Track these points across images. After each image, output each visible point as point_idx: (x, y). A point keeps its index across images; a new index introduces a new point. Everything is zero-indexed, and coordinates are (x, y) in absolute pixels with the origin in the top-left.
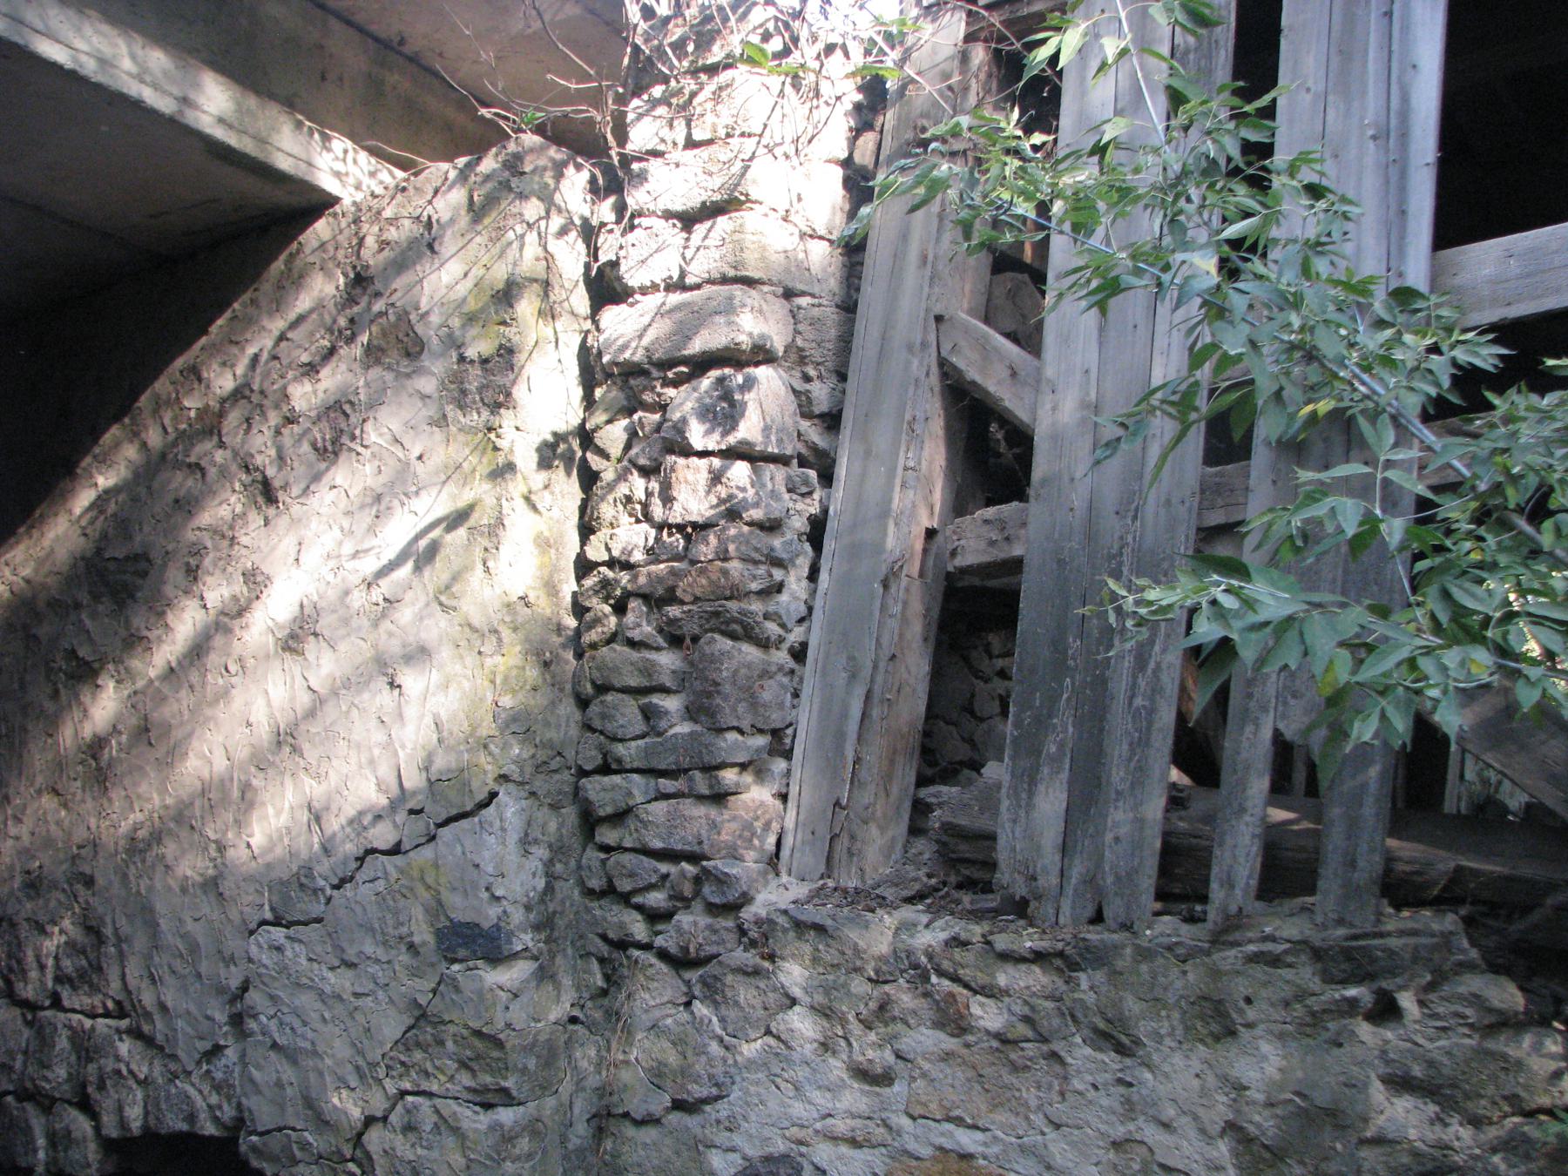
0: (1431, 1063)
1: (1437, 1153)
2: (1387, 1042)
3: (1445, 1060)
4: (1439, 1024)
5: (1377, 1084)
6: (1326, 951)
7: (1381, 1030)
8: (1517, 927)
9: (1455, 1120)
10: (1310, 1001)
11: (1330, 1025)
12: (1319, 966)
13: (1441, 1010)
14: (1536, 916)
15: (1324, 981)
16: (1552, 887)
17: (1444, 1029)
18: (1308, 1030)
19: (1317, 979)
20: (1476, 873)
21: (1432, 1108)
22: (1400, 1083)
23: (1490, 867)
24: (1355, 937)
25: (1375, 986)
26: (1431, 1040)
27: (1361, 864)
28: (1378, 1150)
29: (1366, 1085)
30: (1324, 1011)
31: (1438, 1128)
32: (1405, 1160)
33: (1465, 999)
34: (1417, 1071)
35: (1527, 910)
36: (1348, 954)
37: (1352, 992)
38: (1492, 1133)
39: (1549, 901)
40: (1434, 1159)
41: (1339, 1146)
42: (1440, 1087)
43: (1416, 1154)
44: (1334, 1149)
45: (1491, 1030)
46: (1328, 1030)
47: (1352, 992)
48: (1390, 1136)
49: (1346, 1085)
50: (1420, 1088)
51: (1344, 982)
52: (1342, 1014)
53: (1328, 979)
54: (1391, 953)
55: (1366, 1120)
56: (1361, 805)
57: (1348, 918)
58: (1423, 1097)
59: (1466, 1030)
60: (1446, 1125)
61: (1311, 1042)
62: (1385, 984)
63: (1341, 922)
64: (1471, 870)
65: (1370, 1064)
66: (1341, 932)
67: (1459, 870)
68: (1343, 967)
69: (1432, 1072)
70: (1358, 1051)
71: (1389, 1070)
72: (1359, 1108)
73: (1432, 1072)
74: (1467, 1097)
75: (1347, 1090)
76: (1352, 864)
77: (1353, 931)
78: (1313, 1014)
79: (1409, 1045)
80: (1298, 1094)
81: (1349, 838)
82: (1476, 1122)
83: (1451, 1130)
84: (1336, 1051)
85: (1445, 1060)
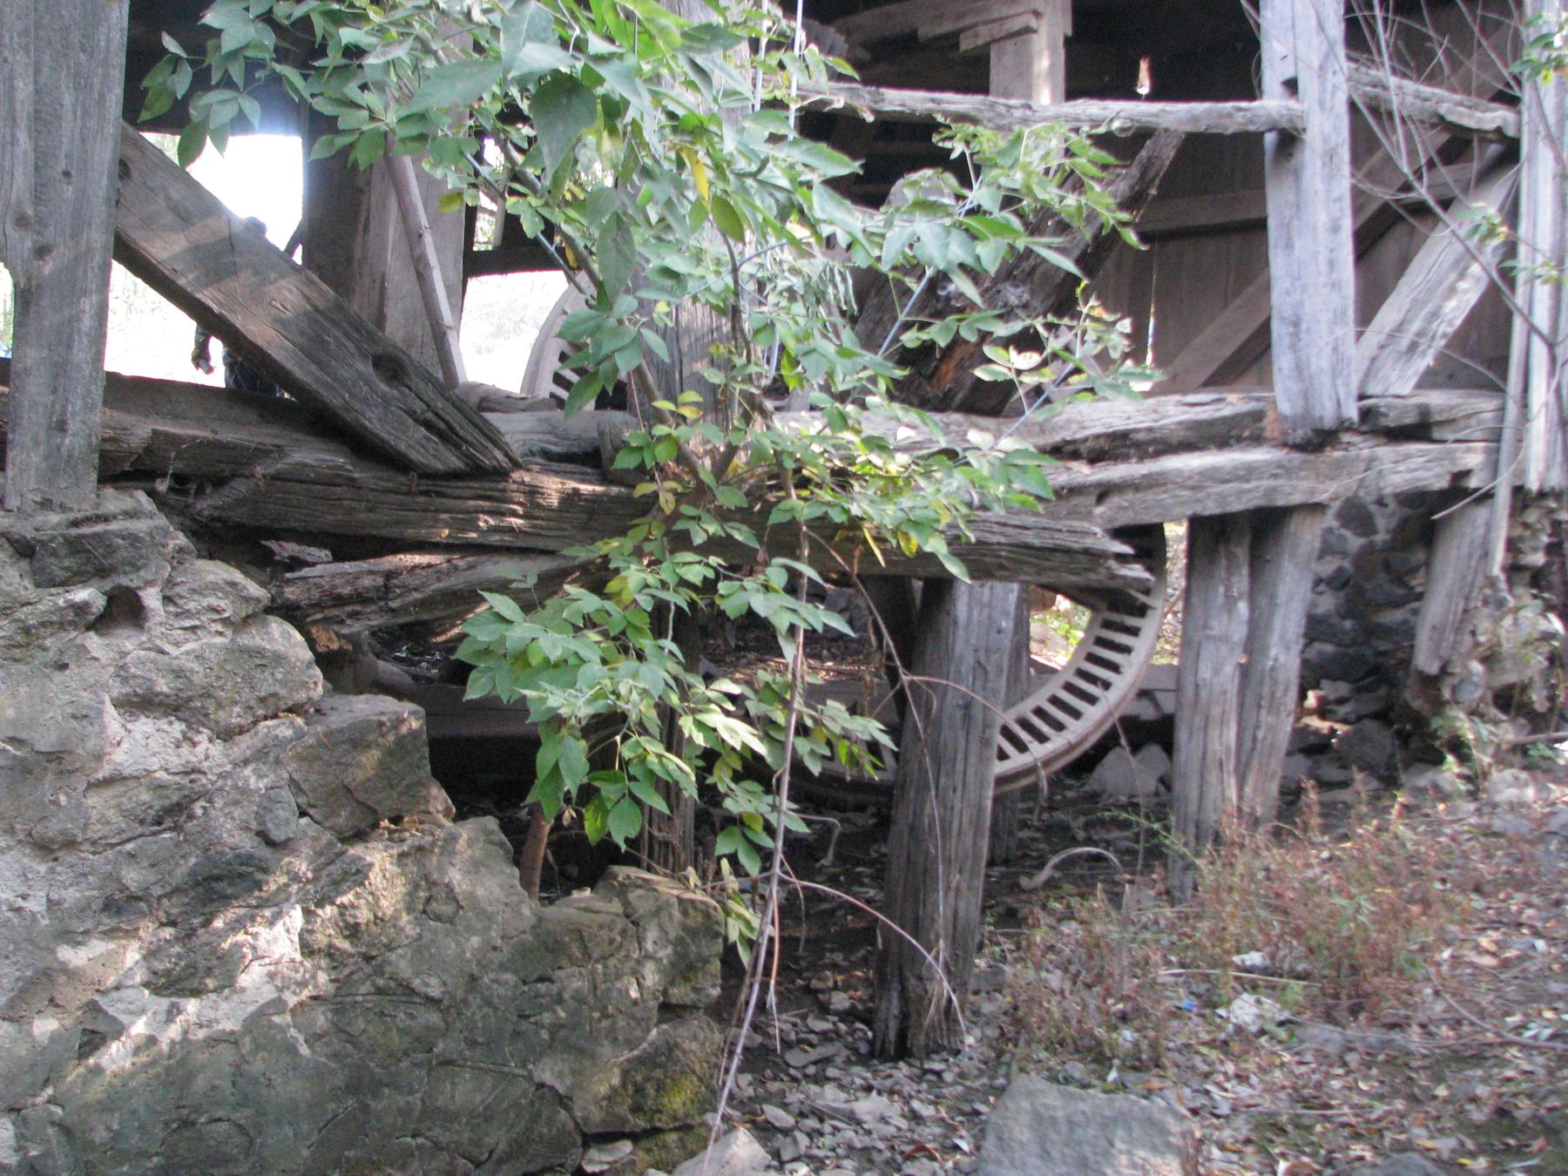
0: (179, 673)
1: (185, 781)
2: (124, 654)
3: (195, 666)
4: (188, 623)
5: (110, 710)
6: (43, 543)
7: (113, 641)
8: (207, 505)
9: (203, 737)
10: (21, 614)
11: (48, 643)
12: (24, 564)
13: (192, 606)
14: (240, 487)
15: (38, 585)
16: (262, 453)
17: (193, 629)
18: (18, 653)
19: (27, 583)
20: (174, 440)
21: (178, 728)
22: (140, 703)
23: (191, 432)
24: (75, 524)
25: (108, 584)
26: (177, 644)
27: (73, 426)
28: (108, 793)
29: (100, 713)
30: (43, 624)
31: (185, 749)
32: (145, 797)
33: (222, 590)
34: (163, 686)
35: (219, 482)
36: (75, 546)
37: (81, 595)
38: (245, 744)
39: (259, 470)
40: (180, 788)
41: (63, 799)
42: (190, 699)
43: (160, 787)
44: (56, 803)
45: (242, 624)
46: (45, 649)
47: (81, 595)
48: (126, 772)
49: (74, 717)
50: (161, 704)
51: (65, 583)
52: (62, 626)
53: (45, 581)
54: (133, 539)
55: (99, 757)
56: (69, 347)
57: (57, 499)
58: (167, 715)
59: (219, 627)
60: (195, 744)
61: (23, 668)
62: (125, 581)
63: (46, 504)
64: (166, 434)
65: (106, 687)
66: (54, 518)
67: (155, 432)
68: (66, 563)
69: (179, 684)
70: (89, 673)
71: (128, 690)
72: (91, 744)
73: (179, 684)
74: (220, 706)
75: (74, 723)
76: (61, 427)
77: (72, 516)
78: (27, 631)
79: (152, 654)
80: (13, 740)
81: (55, 391)
82: (227, 735)
83: (201, 749)
84: (58, 677)
85: (195, 666)
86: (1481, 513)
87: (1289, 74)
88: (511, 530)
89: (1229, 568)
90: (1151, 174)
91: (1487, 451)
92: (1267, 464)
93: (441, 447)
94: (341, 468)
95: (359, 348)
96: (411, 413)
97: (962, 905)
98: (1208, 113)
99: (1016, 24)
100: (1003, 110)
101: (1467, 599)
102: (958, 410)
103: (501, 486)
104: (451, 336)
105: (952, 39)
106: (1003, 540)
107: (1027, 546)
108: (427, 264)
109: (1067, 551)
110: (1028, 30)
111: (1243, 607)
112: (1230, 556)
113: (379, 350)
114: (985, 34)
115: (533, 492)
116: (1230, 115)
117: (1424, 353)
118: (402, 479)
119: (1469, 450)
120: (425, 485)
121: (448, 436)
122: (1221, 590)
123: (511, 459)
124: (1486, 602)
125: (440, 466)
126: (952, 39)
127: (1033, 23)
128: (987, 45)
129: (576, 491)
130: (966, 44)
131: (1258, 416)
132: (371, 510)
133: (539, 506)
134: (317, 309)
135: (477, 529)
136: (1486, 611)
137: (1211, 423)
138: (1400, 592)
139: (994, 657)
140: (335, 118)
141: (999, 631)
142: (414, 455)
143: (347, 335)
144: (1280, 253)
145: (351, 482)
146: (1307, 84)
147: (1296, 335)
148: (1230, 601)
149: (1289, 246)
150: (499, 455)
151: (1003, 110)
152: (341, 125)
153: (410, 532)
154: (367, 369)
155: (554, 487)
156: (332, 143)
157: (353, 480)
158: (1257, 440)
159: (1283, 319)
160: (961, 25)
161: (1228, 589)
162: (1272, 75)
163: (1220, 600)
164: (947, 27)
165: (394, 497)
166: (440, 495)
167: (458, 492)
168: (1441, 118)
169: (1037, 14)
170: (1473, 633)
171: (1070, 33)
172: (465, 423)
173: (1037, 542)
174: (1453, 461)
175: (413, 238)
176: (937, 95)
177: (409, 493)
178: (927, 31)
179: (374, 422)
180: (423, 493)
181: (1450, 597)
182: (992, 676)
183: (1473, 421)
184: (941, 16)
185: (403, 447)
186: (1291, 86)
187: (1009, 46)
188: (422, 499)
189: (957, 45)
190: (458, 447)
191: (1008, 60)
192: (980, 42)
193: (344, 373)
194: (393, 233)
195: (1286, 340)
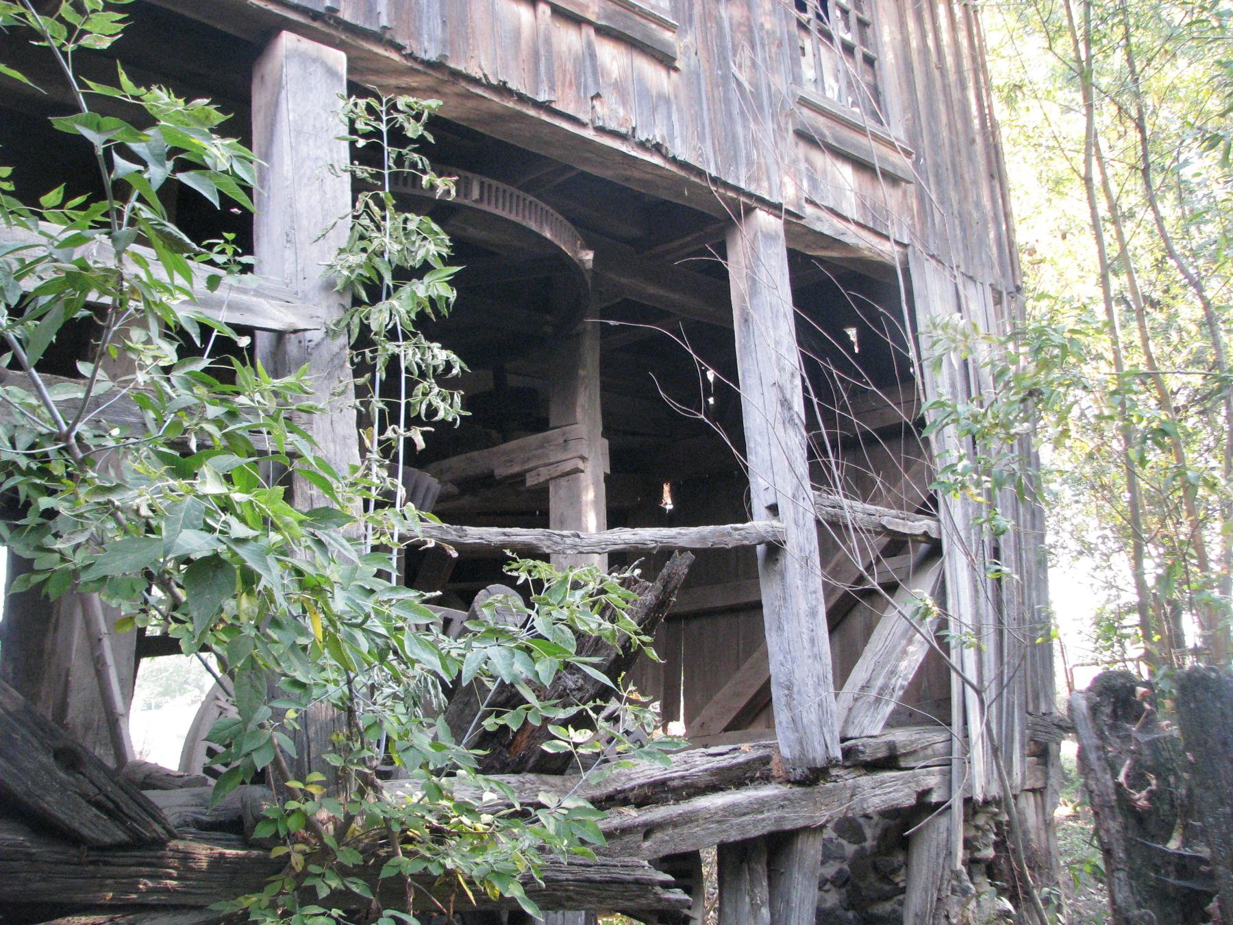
86: (943, 822)
87: (771, 501)
88: (166, 890)
89: (752, 881)
90: (671, 586)
91: (943, 773)
92: (776, 797)
93: (109, 824)
94: (21, 845)
95: (42, 744)
96: (84, 796)
98: (713, 533)
99: (568, 466)
100: (558, 539)
101: (939, 890)
102: (531, 771)
103: (160, 853)
104: (122, 722)
105: (520, 478)
106: (570, 877)
107: (590, 881)
108: (105, 664)
109: (622, 882)
110: (577, 471)
111: (765, 912)
112: (751, 870)
113: (59, 744)
114: (544, 474)
115: (186, 857)
116: (729, 534)
117: (887, 703)
118: (73, 851)
119: (929, 774)
120: (93, 856)
121: (115, 814)
122: (747, 899)
123: (169, 832)
124: (954, 891)
125: (107, 840)
126: (520, 478)
127: (581, 465)
128: (547, 481)
129: (222, 855)
130: (531, 481)
131: (765, 760)
132: (44, 880)
133: (192, 870)
134: (8, 713)
135: (138, 891)
136: (955, 898)
137: (730, 768)
138: (887, 888)
140: (32, 560)
142: (85, 832)
143: (34, 734)
144: (774, 634)
145: (29, 856)
146: (785, 507)
147: (790, 696)
148: (755, 908)
149: (780, 629)
150: (160, 830)
151: (558, 539)
152: (36, 566)
153: (79, 897)
154: (48, 760)
155: (203, 852)
156: (28, 580)
157: (30, 855)
158: (767, 779)
159: (779, 684)
161: (752, 900)
162: (759, 503)
163: (747, 907)
164: (516, 469)
165: (67, 868)
166: (106, 863)
167: (122, 860)
168: (884, 527)
169: (583, 458)
170: (947, 917)
171: (608, 472)
172: (130, 802)
173: (597, 877)
174: (918, 783)
175: (94, 642)
176: (507, 530)
177: (79, 864)
178: (501, 471)
179: (53, 804)
180: (92, 863)
181: (926, 890)
183: (929, 751)
185: (76, 825)
186: (773, 509)
187: (563, 482)
188: (91, 868)
189: (524, 482)
190: (123, 823)
191: (562, 492)
192: (541, 480)
193: (26, 764)
194: (78, 638)
195: (783, 700)
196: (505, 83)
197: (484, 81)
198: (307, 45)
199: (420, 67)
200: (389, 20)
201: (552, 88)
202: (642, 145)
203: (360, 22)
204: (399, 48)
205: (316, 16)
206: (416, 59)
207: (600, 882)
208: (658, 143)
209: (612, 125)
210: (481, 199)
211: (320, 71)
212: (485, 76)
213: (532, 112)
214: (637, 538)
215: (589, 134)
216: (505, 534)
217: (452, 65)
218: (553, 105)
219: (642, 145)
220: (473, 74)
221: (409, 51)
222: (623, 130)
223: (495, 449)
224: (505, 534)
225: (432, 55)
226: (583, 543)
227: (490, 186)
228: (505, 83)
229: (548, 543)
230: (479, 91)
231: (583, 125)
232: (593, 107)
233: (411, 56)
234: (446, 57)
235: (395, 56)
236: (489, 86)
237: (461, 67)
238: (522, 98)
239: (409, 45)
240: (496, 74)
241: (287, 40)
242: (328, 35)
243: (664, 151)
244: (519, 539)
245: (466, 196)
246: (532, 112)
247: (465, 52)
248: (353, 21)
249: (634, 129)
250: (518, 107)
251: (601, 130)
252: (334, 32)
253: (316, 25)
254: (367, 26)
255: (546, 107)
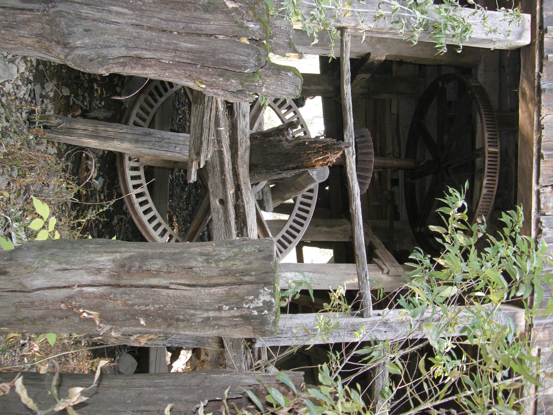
97: (80, 132)
98: (362, 256)
99: (384, 267)
106: (206, 104)
107: (203, 118)
109: (201, 135)
110: (382, 270)
127: (385, 272)
139: (166, 145)
141: (175, 147)
160: (382, 258)
164: (379, 255)
169: (388, 273)
173: (205, 119)
182: (160, 144)
184: (382, 253)
196: (543, 128)
197: (541, 118)
198: (528, 25)
199: (536, 84)
200: (551, 57)
201: (549, 156)
202: (538, 222)
203: (545, 46)
204: (541, 70)
205: (541, 27)
206: (539, 80)
207: (202, 122)
208: (541, 230)
209: (542, 200)
210: (490, 153)
211: (519, 29)
212: (543, 118)
213: (535, 150)
214: (356, 195)
215: (535, 187)
216: (350, 108)
217: (542, 97)
218: (541, 160)
219: (538, 222)
220: (542, 111)
221: (541, 75)
222: (542, 206)
223: (386, 250)
224: (350, 108)
225: (543, 87)
226: (351, 158)
227: (496, 142)
228: (543, 128)
229: (349, 136)
230: (535, 118)
231: (538, 183)
232: (546, 186)
233: (539, 77)
234: (545, 91)
235: (537, 70)
236: (539, 122)
237: (543, 103)
238: (539, 141)
239: (544, 75)
240: (545, 123)
241: (528, 17)
242: (535, 37)
243: (539, 236)
244: (349, 117)
245: (489, 146)
246: (535, 150)
247: (550, 106)
248: (545, 42)
249: (544, 215)
250: (535, 141)
251: (538, 193)
252: (537, 37)
253: (537, 28)
254: (545, 50)
255: (540, 156)
